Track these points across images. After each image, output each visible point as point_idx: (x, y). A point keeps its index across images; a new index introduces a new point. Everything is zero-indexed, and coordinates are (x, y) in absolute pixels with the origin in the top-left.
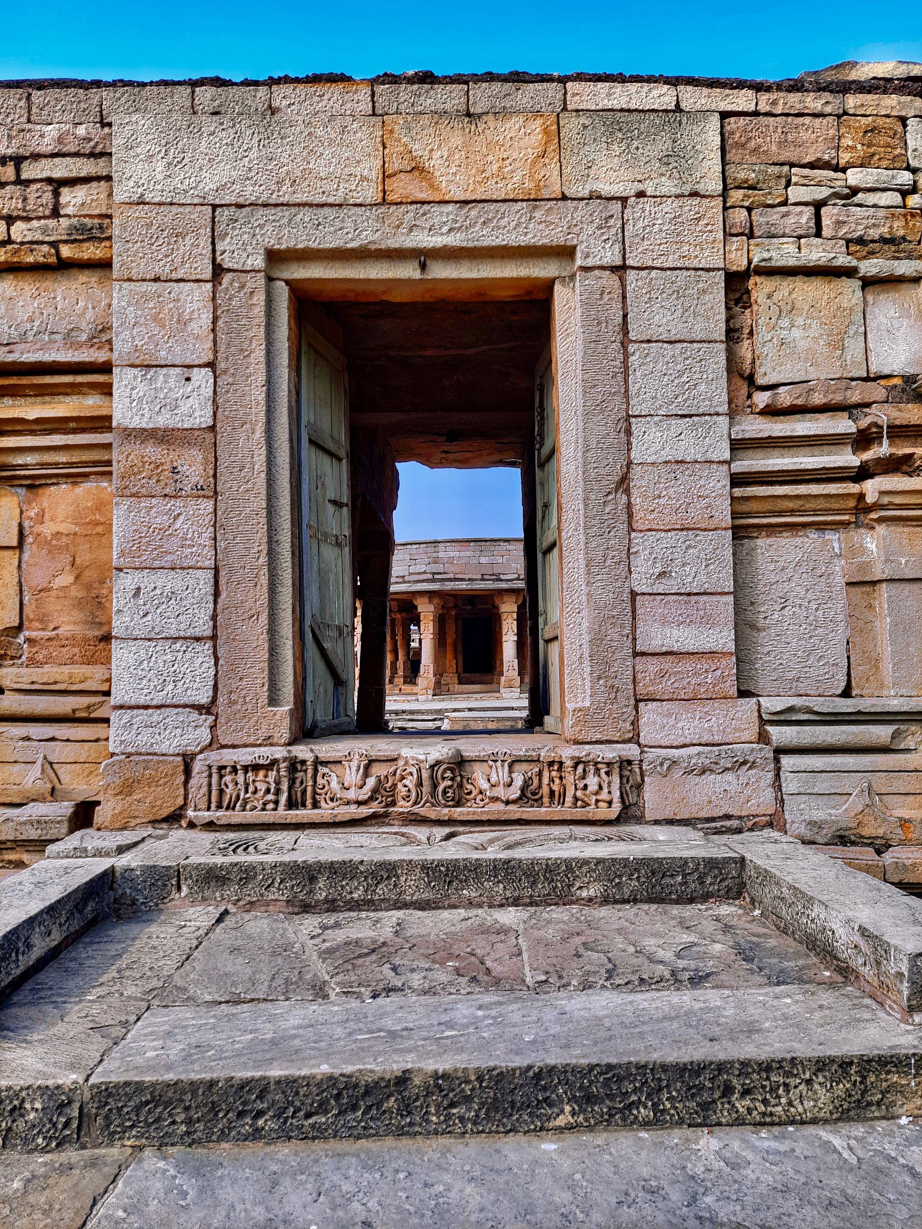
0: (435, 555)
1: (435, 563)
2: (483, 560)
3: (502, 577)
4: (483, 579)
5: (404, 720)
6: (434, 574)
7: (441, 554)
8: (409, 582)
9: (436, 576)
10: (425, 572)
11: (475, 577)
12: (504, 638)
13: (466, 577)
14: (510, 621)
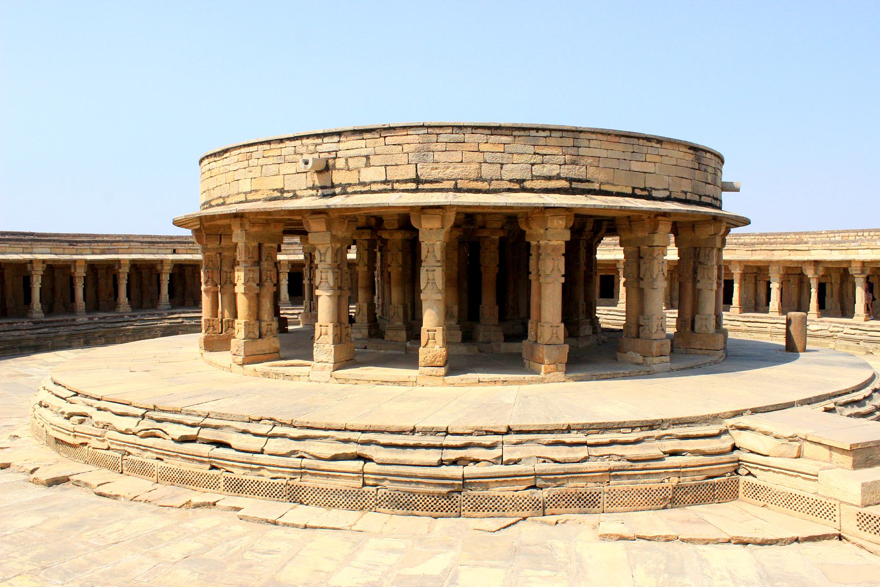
0: (573, 151)
1: (573, 163)
2: (635, 166)
3: (654, 194)
4: (633, 195)
5: (671, 437)
6: (571, 180)
7: (582, 151)
8: (532, 190)
10: (558, 177)
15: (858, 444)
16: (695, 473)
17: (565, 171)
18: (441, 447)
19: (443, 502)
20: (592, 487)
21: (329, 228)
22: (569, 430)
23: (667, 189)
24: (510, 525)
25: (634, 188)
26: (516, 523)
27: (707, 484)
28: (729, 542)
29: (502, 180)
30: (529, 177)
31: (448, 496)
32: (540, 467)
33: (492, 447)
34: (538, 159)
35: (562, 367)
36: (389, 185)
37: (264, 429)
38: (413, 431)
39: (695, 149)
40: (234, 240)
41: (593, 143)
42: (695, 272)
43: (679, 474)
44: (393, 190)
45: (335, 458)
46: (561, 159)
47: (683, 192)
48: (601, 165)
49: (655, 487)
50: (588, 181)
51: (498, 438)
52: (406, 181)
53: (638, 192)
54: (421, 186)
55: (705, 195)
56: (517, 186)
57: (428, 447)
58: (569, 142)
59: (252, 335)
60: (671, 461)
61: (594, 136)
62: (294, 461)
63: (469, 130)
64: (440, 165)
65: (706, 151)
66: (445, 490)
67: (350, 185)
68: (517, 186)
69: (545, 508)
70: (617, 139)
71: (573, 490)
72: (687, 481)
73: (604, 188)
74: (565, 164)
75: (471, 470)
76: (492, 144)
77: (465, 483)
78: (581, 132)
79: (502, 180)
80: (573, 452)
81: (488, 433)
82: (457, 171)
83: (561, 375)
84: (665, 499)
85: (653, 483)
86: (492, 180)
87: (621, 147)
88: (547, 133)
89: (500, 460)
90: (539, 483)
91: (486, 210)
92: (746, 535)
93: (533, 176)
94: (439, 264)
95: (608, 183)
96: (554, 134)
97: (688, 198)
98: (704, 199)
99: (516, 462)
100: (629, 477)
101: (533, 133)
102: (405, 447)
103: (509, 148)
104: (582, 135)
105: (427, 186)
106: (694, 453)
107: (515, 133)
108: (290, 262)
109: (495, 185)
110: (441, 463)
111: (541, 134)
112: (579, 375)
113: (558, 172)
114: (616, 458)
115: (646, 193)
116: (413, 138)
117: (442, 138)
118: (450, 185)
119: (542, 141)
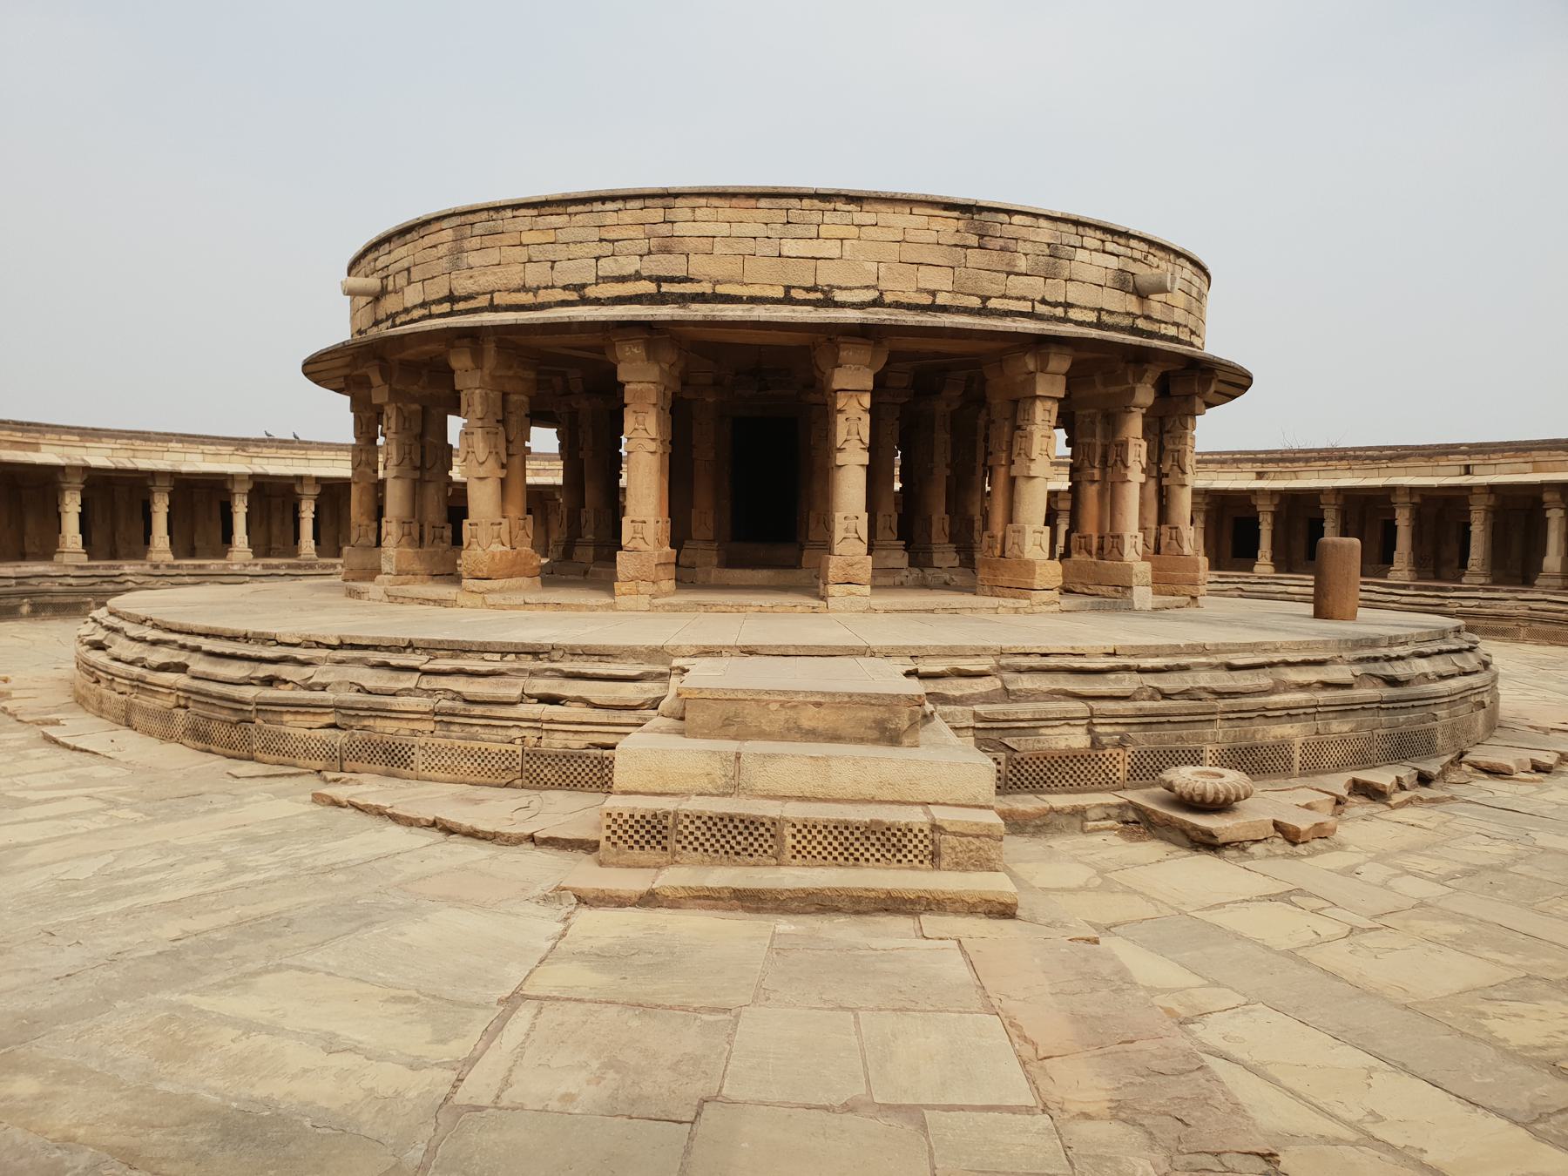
0: (665, 229)
2: (790, 248)
3: (839, 296)
4: (788, 300)
6: (658, 280)
7: (679, 229)
8: (597, 302)
9: (665, 288)
10: (637, 277)
12: (840, 459)
15: (701, 690)
16: (570, 736)
21: (386, 375)
22: (411, 646)
25: (788, 289)
29: (553, 287)
34: (607, 248)
37: (152, 634)
38: (246, 638)
39: (967, 209)
44: (431, 316)
46: (643, 246)
47: (919, 290)
49: (495, 747)
50: (691, 280)
51: (324, 653)
52: (439, 302)
53: (795, 294)
54: (458, 307)
55: (1004, 296)
56: (574, 296)
58: (658, 215)
61: (703, 201)
62: (136, 671)
64: (475, 272)
66: (235, 719)
67: (397, 313)
68: (574, 296)
69: (342, 760)
70: (752, 202)
73: (720, 289)
74: (650, 253)
75: (281, 693)
78: (677, 195)
80: (398, 680)
81: (319, 644)
85: (493, 742)
86: (538, 288)
87: (761, 215)
88: (619, 205)
92: (451, 815)
93: (597, 277)
94: (479, 423)
97: (939, 301)
98: (993, 304)
101: (598, 206)
103: (562, 236)
104: (680, 202)
105: (461, 306)
107: (572, 209)
109: (543, 296)
111: (610, 206)
113: (638, 267)
114: (450, 695)
115: (819, 295)
117: (478, 229)
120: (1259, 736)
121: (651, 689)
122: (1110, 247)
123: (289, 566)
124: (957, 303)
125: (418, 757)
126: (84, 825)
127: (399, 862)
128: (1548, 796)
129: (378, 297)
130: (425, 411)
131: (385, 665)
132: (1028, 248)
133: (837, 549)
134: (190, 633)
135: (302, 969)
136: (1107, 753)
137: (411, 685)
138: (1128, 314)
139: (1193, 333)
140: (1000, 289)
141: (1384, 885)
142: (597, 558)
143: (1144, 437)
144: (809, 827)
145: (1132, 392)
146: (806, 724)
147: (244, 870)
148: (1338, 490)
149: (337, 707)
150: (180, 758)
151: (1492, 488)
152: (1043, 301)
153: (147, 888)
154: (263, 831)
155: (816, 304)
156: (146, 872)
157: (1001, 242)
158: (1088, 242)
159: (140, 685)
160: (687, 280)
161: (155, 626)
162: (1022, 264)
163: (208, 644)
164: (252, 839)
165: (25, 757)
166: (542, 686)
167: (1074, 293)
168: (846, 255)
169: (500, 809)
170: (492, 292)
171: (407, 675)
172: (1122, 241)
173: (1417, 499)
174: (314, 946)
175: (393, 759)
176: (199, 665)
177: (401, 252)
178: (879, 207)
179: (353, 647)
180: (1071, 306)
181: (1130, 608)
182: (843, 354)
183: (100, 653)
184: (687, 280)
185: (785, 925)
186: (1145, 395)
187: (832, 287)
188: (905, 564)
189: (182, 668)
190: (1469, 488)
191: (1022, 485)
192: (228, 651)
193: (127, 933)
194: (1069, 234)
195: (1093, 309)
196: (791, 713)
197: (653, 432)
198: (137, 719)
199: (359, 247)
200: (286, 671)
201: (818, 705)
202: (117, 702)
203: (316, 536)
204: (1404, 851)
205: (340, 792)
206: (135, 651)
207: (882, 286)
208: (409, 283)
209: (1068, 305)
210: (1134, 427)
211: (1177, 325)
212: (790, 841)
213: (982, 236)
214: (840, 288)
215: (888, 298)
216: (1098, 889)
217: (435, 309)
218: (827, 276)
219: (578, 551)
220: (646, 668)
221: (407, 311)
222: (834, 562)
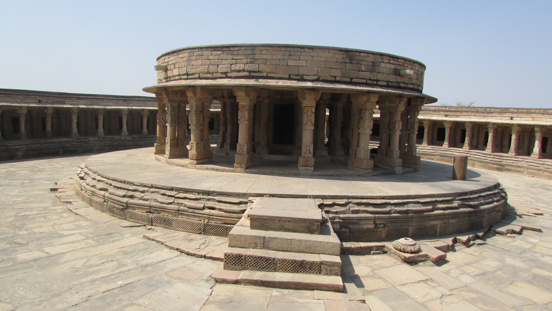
0: (252, 56)
1: (252, 63)
2: (291, 63)
3: (305, 78)
4: (290, 79)
5: (214, 200)
6: (250, 72)
7: (257, 57)
8: (231, 78)
9: (252, 74)
10: (243, 71)
11: (283, 76)
12: (304, 127)
13: (276, 76)
14: (309, 113)
17: (247, 67)
18: (129, 190)
19: (122, 212)
20: (170, 216)
21: (168, 95)
22: (172, 189)
23: (317, 75)
24: (135, 226)
26: (139, 226)
27: (223, 227)
28: (177, 249)
29: (218, 72)
30: (229, 70)
31: (122, 210)
32: (154, 204)
33: (143, 192)
34: (234, 61)
35: (244, 166)
36: (180, 77)
38: (125, 182)
39: (346, 51)
40: (164, 102)
41: (263, 52)
42: (359, 123)
43: (209, 219)
44: (181, 79)
45: (101, 189)
46: (245, 61)
47: (331, 76)
48: (268, 63)
49: (196, 222)
51: (146, 189)
53: (292, 77)
55: (357, 78)
56: (224, 76)
57: (124, 189)
59: (160, 142)
60: (207, 211)
61: (264, 48)
62: (93, 189)
63: (205, 49)
64: (194, 67)
65: (360, 52)
66: (121, 207)
68: (224, 76)
69: (152, 222)
70: (279, 49)
71: (162, 216)
72: (213, 223)
73: (269, 75)
74: (247, 63)
76: (213, 56)
77: (127, 206)
79: (218, 72)
80: (168, 199)
81: (146, 186)
82: (200, 69)
83: (243, 170)
84: (200, 229)
85: (195, 220)
86: (213, 73)
89: (141, 199)
90: (152, 211)
91: (218, 88)
92: (182, 248)
95: (272, 73)
96: (241, 49)
98: (354, 80)
99: (147, 200)
100: (187, 215)
101: (232, 49)
102: (118, 188)
103: (221, 57)
104: (257, 48)
105: (190, 77)
106: (220, 210)
107: (224, 49)
108: (27, 107)
109: (215, 75)
110: (124, 196)
112: (252, 170)
115: (299, 77)
116: (186, 54)
118: (197, 76)
119: (236, 53)
120: (427, 224)
121: (242, 207)
122: (392, 62)
123: (139, 138)
124: (342, 80)
125: (174, 223)
126: (79, 246)
127: (167, 264)
128: (516, 243)
129: (166, 70)
130: (179, 105)
131: (164, 195)
132: (365, 63)
133: (303, 155)
134: (109, 179)
135: (138, 305)
136: (379, 230)
137: (172, 201)
138: (397, 82)
139: (419, 86)
140: (355, 76)
141: (457, 278)
142: (231, 149)
143: (402, 120)
144: (284, 261)
145: (397, 106)
146: (286, 227)
147: (124, 265)
148: (471, 122)
149: (151, 207)
150: (106, 217)
151: (519, 125)
152: (370, 79)
153: (97, 272)
154: (129, 250)
155: (298, 80)
156: (97, 266)
157: (357, 61)
158: (385, 61)
159: (93, 193)
160: (259, 72)
161: (98, 175)
162: (363, 68)
163: (114, 183)
164: (126, 253)
165: (62, 217)
166: (210, 204)
167: (379, 77)
168: (308, 65)
169: (196, 242)
170: (199, 73)
171: (170, 198)
172: (396, 60)
173: (495, 127)
174: (142, 297)
175: (167, 224)
176: (111, 190)
177: (172, 58)
178: (318, 51)
179: (156, 188)
180: (379, 81)
181: (394, 173)
182: (306, 96)
183: (83, 181)
184: (259, 72)
185: (275, 292)
186: (402, 108)
187: (303, 75)
188: (327, 154)
189: (106, 190)
190: (512, 125)
191: (362, 136)
192: (120, 186)
193: (91, 289)
194: (379, 59)
195: (385, 81)
196: (282, 223)
197: (247, 117)
198: (93, 204)
199: (160, 55)
200: (136, 194)
201: (290, 221)
202: (88, 198)
203: (148, 128)
204: (466, 264)
205: (151, 234)
206: (94, 183)
207: (319, 75)
208: (175, 68)
209: (377, 80)
210: (398, 117)
211: (413, 84)
212: (279, 265)
213: (351, 60)
214: (306, 75)
215: (321, 79)
216: (371, 276)
217: (182, 77)
218: (301, 73)
219: (225, 146)
220: (241, 200)
221: (174, 76)
222: (301, 160)
